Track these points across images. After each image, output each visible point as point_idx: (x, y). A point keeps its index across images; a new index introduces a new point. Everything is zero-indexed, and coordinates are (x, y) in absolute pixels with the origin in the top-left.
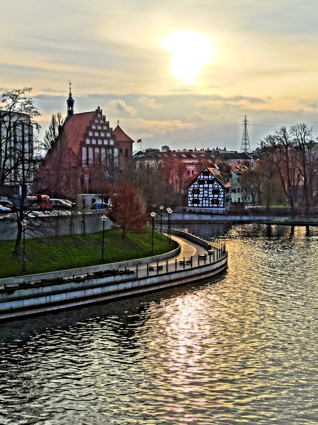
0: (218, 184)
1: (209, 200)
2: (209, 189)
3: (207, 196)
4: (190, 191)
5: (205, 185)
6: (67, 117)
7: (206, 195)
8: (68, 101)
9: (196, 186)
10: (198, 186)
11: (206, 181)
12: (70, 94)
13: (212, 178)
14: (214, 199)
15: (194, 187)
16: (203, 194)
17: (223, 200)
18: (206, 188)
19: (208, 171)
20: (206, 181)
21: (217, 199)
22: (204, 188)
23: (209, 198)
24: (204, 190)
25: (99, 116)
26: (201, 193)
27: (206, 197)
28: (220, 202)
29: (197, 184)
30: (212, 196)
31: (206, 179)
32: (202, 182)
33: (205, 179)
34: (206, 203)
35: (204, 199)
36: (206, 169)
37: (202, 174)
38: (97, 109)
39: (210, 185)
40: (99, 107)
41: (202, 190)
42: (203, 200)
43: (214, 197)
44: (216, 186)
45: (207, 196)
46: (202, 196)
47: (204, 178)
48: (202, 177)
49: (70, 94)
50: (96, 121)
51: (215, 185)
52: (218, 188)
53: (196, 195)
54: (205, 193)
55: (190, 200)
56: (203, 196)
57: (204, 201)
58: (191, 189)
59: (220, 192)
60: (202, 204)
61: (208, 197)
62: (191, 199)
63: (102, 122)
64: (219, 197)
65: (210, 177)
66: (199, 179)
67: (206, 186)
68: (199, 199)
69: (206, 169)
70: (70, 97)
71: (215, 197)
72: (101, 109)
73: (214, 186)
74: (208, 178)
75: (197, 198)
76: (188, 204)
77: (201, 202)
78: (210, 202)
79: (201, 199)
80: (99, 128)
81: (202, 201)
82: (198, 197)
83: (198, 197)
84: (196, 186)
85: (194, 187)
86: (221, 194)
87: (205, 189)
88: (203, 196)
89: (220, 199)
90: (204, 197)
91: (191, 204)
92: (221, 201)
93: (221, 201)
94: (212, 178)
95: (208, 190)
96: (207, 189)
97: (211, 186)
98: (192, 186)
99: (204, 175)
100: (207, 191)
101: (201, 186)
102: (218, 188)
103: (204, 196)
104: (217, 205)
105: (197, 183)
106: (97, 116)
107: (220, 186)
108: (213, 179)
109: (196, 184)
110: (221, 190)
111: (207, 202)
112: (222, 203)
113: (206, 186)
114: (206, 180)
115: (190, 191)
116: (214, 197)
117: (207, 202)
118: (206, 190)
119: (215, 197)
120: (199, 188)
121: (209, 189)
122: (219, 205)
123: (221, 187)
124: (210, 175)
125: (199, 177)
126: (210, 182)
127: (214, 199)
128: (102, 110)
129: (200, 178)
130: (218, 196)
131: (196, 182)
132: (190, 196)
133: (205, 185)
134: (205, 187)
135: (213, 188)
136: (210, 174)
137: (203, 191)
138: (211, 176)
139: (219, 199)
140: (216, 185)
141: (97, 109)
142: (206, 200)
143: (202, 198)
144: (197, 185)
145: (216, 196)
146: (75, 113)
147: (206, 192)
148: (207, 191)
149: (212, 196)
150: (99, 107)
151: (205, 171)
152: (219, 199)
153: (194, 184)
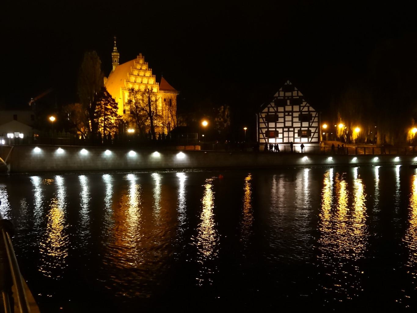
0: (308, 105)
1: (294, 131)
2: (294, 114)
3: (291, 125)
4: (262, 118)
5: (286, 107)
7: (288, 124)
9: (271, 110)
10: (275, 109)
11: (288, 102)
13: (298, 96)
14: (302, 129)
15: (269, 112)
16: (284, 123)
17: (317, 131)
18: (289, 112)
19: (291, 84)
20: (288, 102)
21: (307, 129)
22: (285, 112)
23: (294, 128)
24: (285, 115)
26: (281, 120)
27: (289, 127)
28: (312, 134)
29: (273, 105)
30: (299, 125)
31: (288, 97)
32: (282, 103)
33: (286, 98)
34: (288, 137)
35: (286, 129)
36: (288, 82)
37: (281, 89)
39: (294, 107)
41: (283, 116)
42: (283, 131)
43: (301, 127)
44: (306, 109)
45: (291, 125)
46: (282, 125)
47: (284, 96)
48: (282, 94)
51: (304, 107)
52: (309, 111)
53: (272, 125)
54: (286, 120)
55: (263, 134)
56: (285, 125)
57: (286, 134)
58: (264, 115)
59: (313, 118)
60: (283, 138)
61: (292, 127)
62: (264, 131)
64: (310, 126)
65: (295, 93)
66: (277, 97)
67: (288, 108)
68: (277, 129)
69: (288, 82)
71: (303, 126)
73: (302, 108)
74: (292, 96)
75: (274, 129)
76: (259, 138)
77: (280, 136)
78: (296, 135)
79: (280, 131)
80: (142, 74)
81: (283, 133)
82: (276, 128)
83: (276, 128)
84: (271, 110)
85: (269, 112)
86: (312, 122)
87: (287, 114)
88: (285, 125)
89: (313, 130)
90: (285, 127)
91: (264, 138)
92: (314, 133)
93: (314, 133)
94: (298, 96)
95: (292, 115)
96: (290, 114)
97: (296, 108)
98: (266, 110)
99: (285, 91)
100: (291, 117)
101: (281, 109)
102: (309, 111)
103: (286, 125)
104: (308, 140)
105: (273, 104)
106: (138, 63)
107: (311, 109)
108: (300, 96)
109: (272, 107)
110: (314, 114)
111: (291, 134)
112: (316, 135)
113: (288, 108)
114: (288, 99)
115: (262, 118)
116: (301, 127)
117: (291, 134)
118: (289, 115)
119: (303, 126)
120: (277, 112)
121: (294, 114)
122: (310, 139)
123: (314, 110)
124: (294, 91)
125: (277, 95)
126: (294, 102)
127: (302, 129)
129: (279, 96)
130: (309, 124)
131: (271, 103)
132: (262, 125)
133: (286, 107)
134: (286, 110)
135: (300, 111)
136: (296, 89)
137: (284, 118)
138: (296, 92)
139: (310, 129)
140: (305, 106)
142: (289, 131)
143: (283, 128)
144: (273, 107)
145: (305, 124)
147: (288, 118)
148: (291, 117)
149: (299, 125)
151: (286, 84)
152: (310, 129)
153: (269, 106)
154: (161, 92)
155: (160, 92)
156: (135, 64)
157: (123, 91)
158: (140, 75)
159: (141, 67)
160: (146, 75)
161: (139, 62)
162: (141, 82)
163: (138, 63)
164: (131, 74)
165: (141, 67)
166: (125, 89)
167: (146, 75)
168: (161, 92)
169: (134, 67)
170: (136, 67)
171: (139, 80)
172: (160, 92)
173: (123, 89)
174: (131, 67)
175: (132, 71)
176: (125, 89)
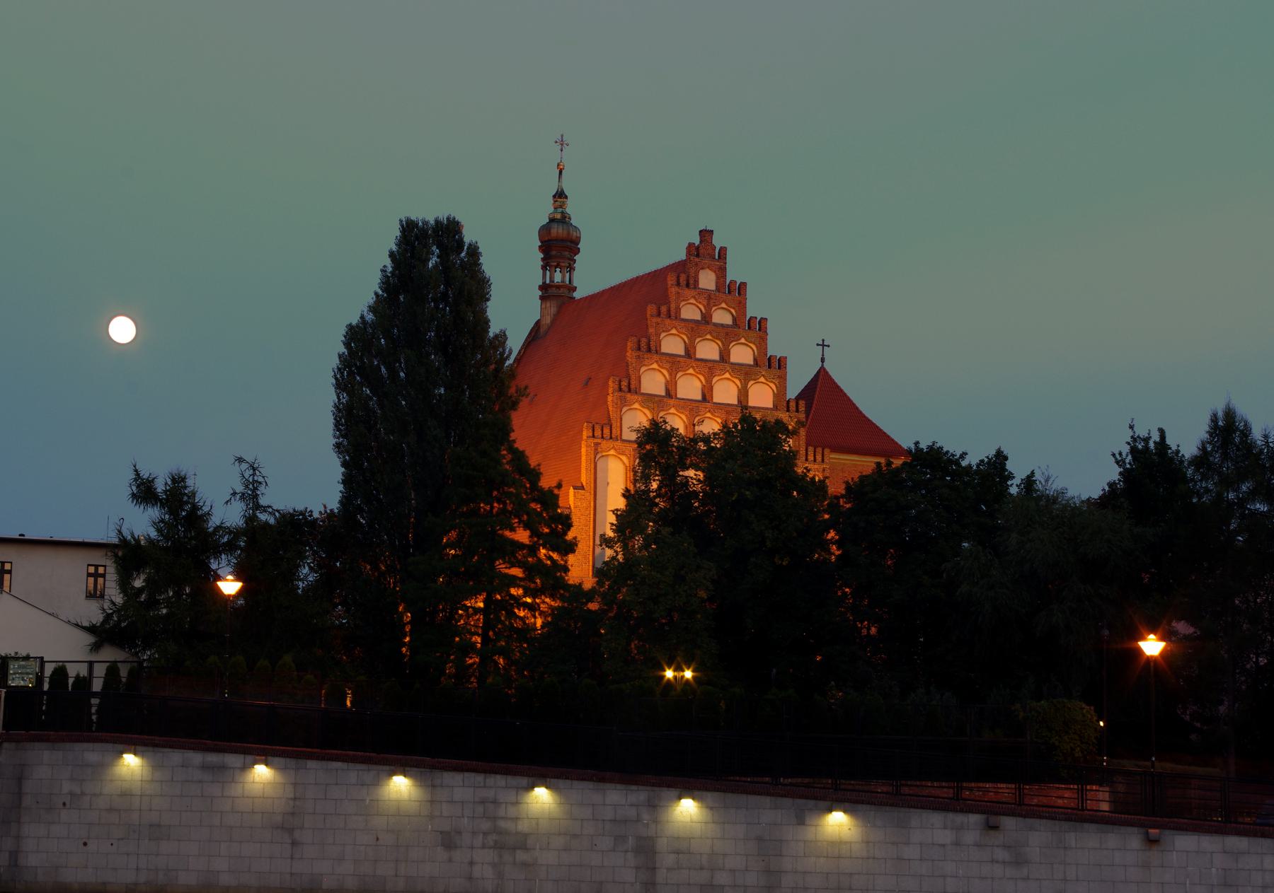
6: (538, 323)
8: (544, 232)
12: (560, 195)
25: (707, 280)
38: (697, 241)
40: (706, 234)
49: (560, 195)
50: (690, 312)
63: (722, 317)
70: (561, 219)
72: (718, 241)
80: (708, 350)
106: (692, 283)
128: (723, 251)
141: (697, 241)
146: (577, 295)
150: (706, 234)
154: (819, 458)
155: (811, 458)
156: (673, 290)
157: (597, 444)
158: (698, 356)
159: (708, 307)
160: (734, 359)
161: (696, 281)
162: (699, 398)
163: (688, 285)
164: (650, 349)
165: (708, 307)
166: (607, 431)
167: (734, 359)
168: (819, 458)
169: (664, 309)
170: (678, 310)
171: (690, 387)
172: (811, 458)
173: (598, 433)
174: (651, 309)
175: (651, 330)
176: (607, 431)
